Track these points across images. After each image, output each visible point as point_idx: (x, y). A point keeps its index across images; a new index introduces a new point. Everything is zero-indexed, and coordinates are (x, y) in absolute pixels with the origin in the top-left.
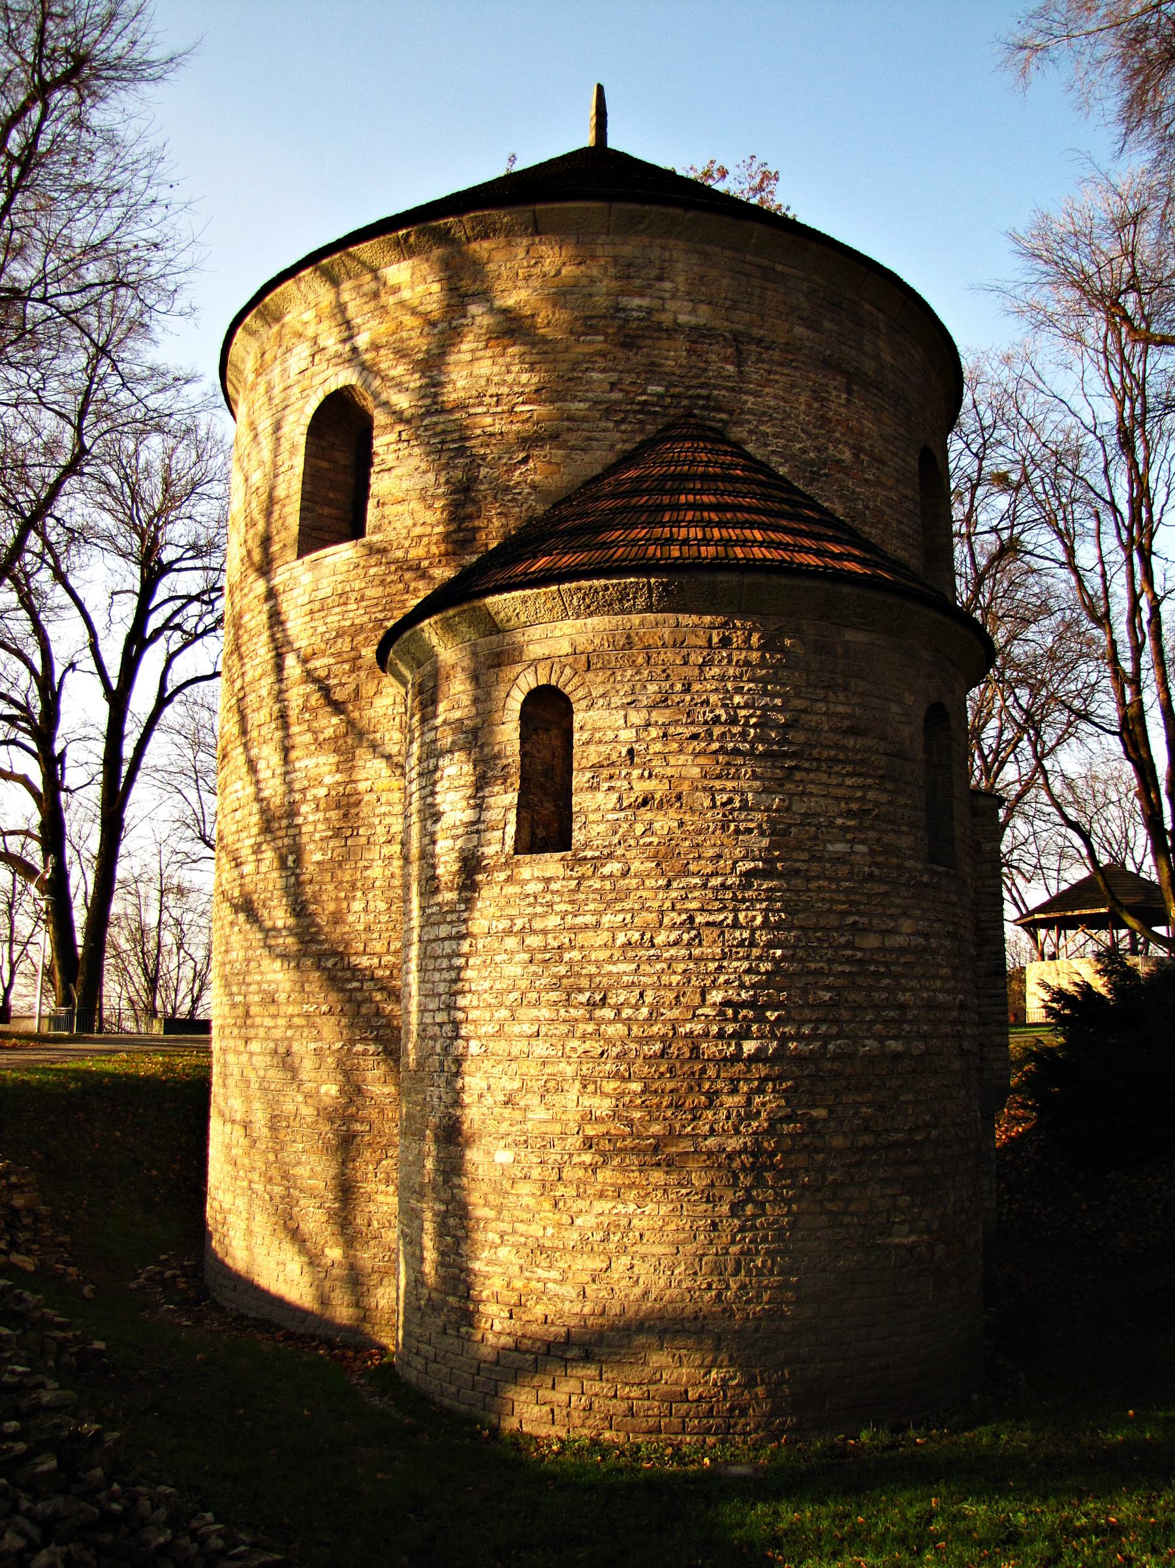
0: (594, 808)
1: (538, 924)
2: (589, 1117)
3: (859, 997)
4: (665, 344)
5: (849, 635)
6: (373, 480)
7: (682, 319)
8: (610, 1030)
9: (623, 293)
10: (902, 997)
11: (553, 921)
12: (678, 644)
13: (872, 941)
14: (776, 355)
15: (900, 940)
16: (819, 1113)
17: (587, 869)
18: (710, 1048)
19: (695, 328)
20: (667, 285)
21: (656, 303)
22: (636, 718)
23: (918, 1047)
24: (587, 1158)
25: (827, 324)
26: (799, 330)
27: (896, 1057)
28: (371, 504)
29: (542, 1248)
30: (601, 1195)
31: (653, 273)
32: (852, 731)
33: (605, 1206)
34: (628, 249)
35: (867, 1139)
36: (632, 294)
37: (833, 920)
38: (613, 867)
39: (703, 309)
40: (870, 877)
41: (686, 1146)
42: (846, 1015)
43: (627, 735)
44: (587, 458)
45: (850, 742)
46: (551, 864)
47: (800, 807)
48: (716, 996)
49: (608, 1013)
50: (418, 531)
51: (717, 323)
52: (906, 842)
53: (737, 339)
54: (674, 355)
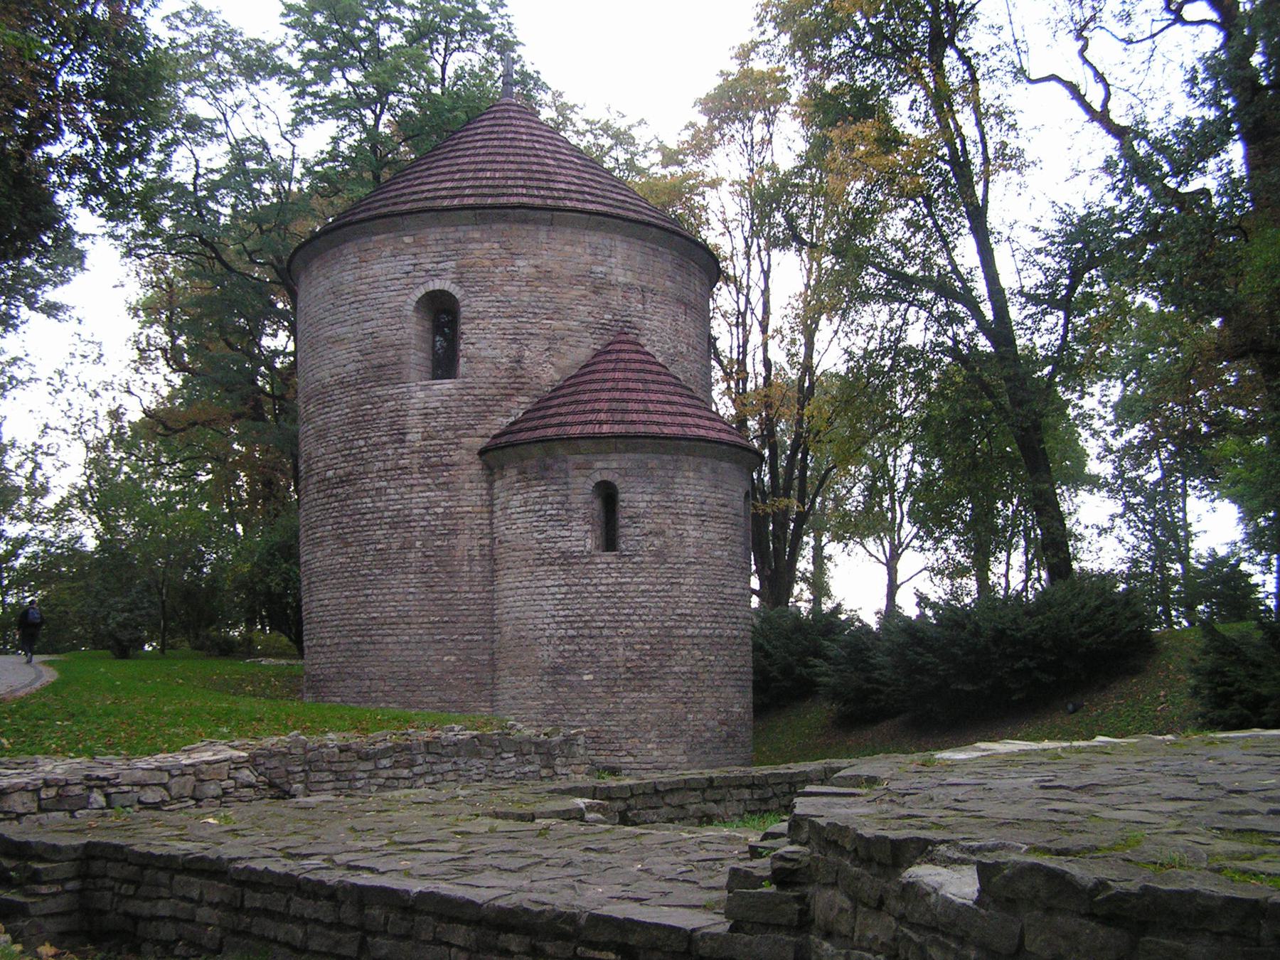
0: (629, 535)
1: (604, 581)
2: (627, 660)
3: (724, 613)
4: (612, 292)
5: (725, 465)
6: (462, 347)
7: (621, 279)
8: (637, 625)
9: (593, 263)
10: (738, 614)
11: (610, 581)
12: (662, 468)
13: (728, 591)
14: (658, 298)
15: (736, 591)
16: (712, 658)
17: (627, 559)
18: (676, 632)
19: (625, 285)
20: (613, 260)
21: (609, 270)
22: (647, 498)
23: (742, 634)
24: (629, 675)
25: (679, 278)
26: (668, 283)
27: (735, 637)
28: (462, 361)
29: (608, 713)
30: (634, 690)
31: (607, 253)
32: (723, 505)
33: (636, 694)
34: (595, 238)
35: (727, 669)
36: (598, 264)
37: (717, 582)
38: (637, 559)
39: (629, 273)
40: (728, 565)
41: (667, 670)
42: (720, 619)
43: (642, 505)
44: (579, 351)
45: (722, 509)
46: (609, 557)
47: (706, 537)
48: (679, 611)
49: (635, 618)
50: (492, 380)
51: (635, 282)
52: (739, 550)
53: (643, 290)
54: (616, 299)
